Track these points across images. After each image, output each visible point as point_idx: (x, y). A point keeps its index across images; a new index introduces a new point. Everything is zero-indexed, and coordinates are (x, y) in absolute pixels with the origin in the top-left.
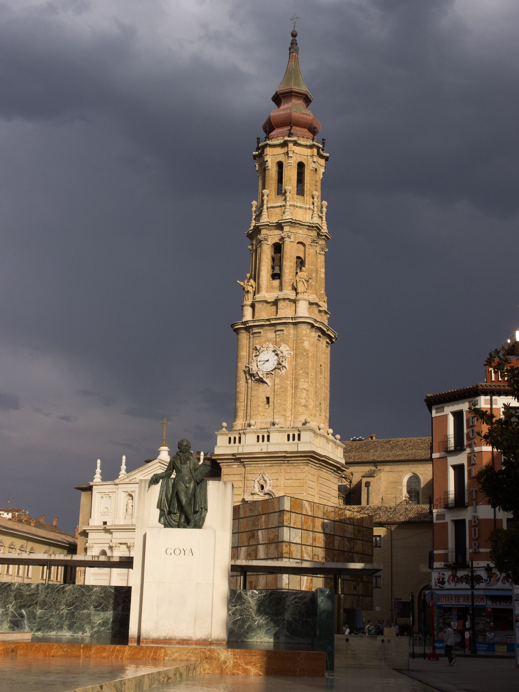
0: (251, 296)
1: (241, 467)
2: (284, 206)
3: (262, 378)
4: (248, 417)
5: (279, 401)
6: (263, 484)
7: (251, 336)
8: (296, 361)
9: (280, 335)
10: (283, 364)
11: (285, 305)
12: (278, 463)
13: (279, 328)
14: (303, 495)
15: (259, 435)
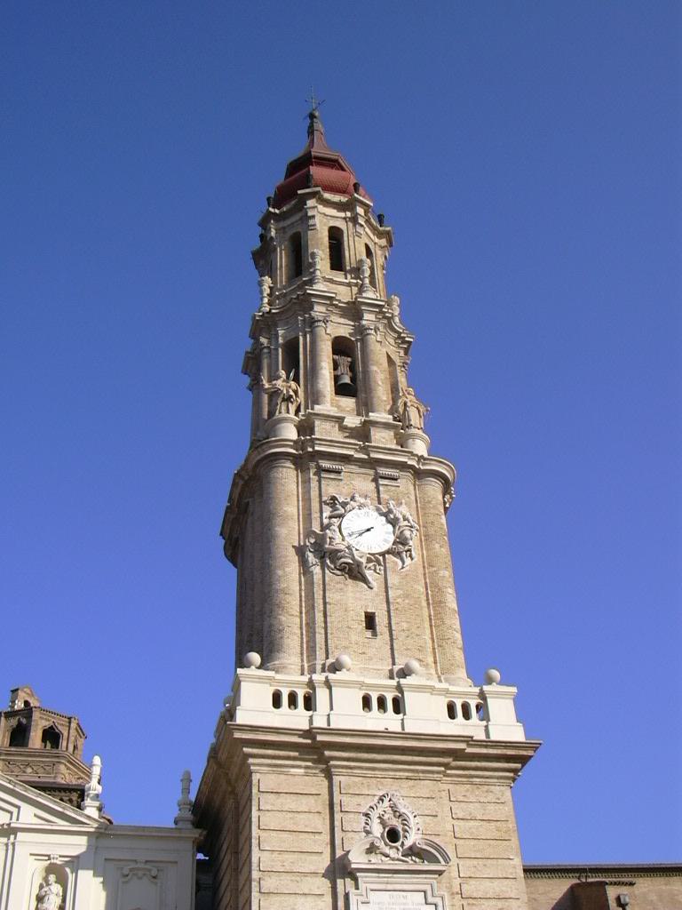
0: (292, 408)
1: (315, 775)
2: (356, 285)
3: (359, 564)
4: (320, 654)
5: (405, 625)
6: (394, 823)
7: (314, 478)
8: (427, 550)
9: (389, 487)
10: (411, 543)
11: (387, 438)
12: (432, 772)
13: (383, 471)
14: (511, 862)
15: (370, 693)
